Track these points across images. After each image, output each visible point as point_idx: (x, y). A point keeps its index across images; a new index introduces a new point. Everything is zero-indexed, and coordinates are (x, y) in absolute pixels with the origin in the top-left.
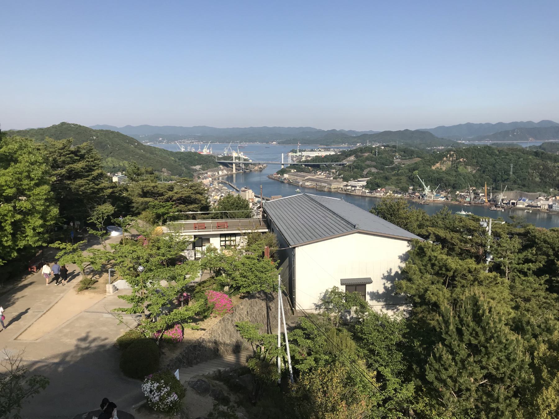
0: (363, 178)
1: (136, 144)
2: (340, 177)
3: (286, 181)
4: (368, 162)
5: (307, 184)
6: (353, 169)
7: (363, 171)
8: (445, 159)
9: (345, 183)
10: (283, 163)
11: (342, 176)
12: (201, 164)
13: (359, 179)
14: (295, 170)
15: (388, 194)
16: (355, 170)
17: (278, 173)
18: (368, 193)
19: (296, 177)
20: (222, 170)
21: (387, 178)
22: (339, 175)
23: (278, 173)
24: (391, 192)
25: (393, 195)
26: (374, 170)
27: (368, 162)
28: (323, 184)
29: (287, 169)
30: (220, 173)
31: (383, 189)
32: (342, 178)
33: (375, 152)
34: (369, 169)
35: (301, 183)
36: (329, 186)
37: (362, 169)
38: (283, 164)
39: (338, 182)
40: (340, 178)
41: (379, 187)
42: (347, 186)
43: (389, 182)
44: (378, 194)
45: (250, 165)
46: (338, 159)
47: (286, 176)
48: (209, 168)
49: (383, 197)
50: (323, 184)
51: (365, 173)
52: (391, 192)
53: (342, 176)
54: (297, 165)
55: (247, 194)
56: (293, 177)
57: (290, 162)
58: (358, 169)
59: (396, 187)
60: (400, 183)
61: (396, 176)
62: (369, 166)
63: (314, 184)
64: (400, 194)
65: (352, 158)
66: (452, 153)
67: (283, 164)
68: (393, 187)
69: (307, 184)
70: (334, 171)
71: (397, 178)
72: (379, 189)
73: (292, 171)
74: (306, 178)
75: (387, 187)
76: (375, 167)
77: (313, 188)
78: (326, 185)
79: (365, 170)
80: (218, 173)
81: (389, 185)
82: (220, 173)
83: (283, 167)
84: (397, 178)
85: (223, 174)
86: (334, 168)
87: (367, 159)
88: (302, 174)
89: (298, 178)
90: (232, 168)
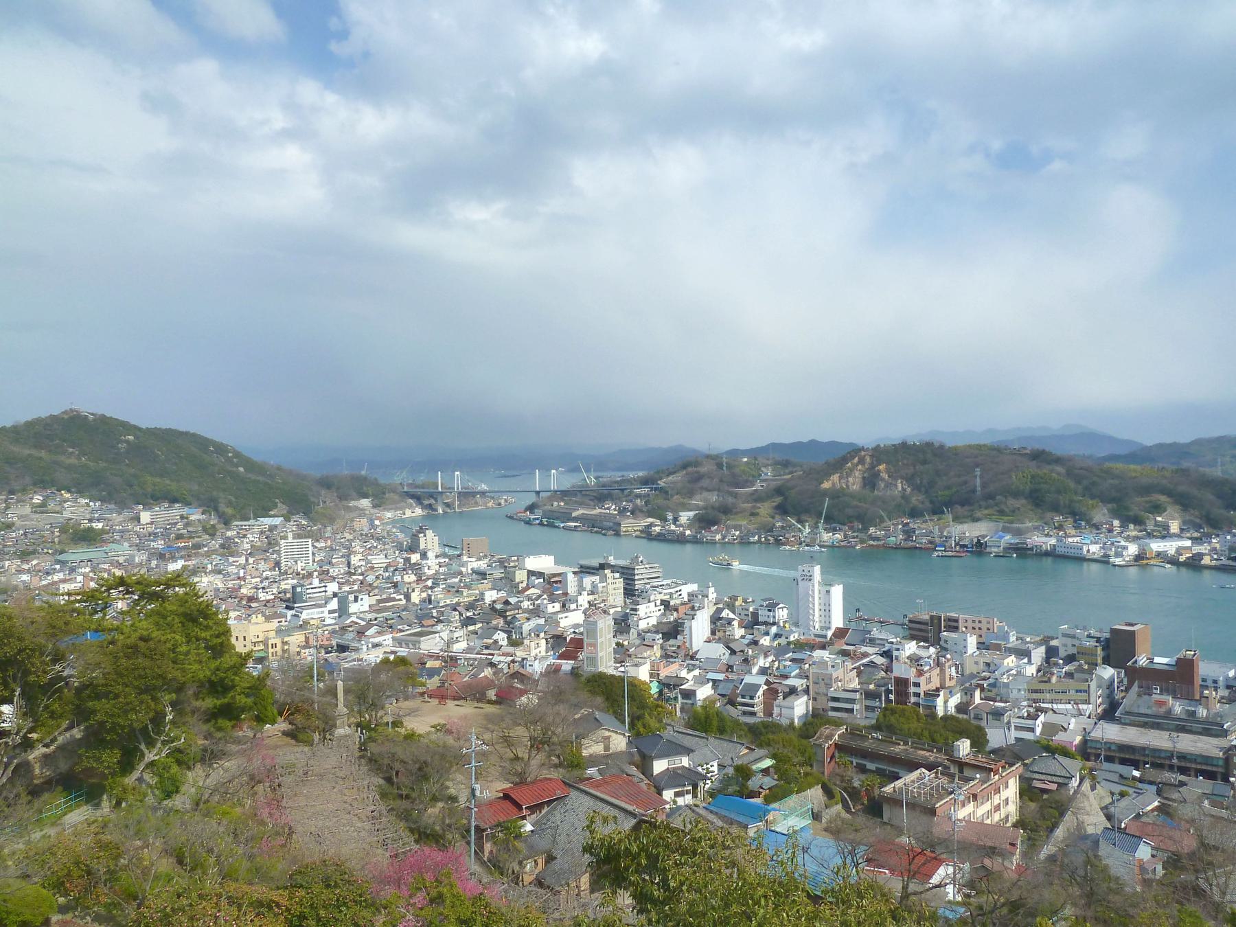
1: (230, 455)
10: (538, 489)
14: (562, 504)
20: (410, 507)
55: (422, 540)
66: (863, 453)
67: (538, 493)
74: (574, 515)
85: (414, 515)
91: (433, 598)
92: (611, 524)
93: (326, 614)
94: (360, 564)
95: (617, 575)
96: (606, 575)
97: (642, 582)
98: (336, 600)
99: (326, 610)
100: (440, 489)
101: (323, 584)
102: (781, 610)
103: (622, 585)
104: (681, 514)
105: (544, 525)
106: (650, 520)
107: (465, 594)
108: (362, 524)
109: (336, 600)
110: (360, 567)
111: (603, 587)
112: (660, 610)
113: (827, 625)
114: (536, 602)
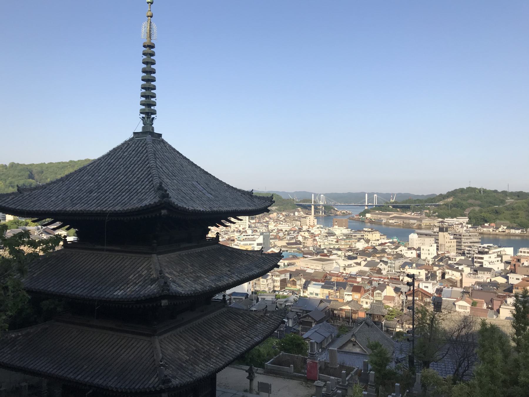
0: (462, 216)
2: (435, 215)
3: (367, 221)
4: (470, 201)
5: (391, 221)
6: (451, 207)
7: (464, 210)
9: (440, 220)
11: (437, 213)
12: (279, 205)
13: (458, 218)
15: (500, 230)
16: (454, 209)
17: (360, 215)
18: (470, 228)
19: (379, 216)
20: (298, 211)
21: (497, 212)
22: (434, 213)
23: (360, 215)
24: (505, 227)
25: (507, 231)
26: (477, 209)
27: (470, 201)
28: (412, 221)
29: (371, 210)
30: (296, 214)
31: (493, 224)
32: (437, 216)
33: (480, 192)
34: (472, 208)
35: (384, 221)
36: (419, 223)
38: (367, 206)
39: (431, 218)
40: (434, 216)
41: (487, 222)
42: (442, 222)
43: (500, 217)
44: (485, 229)
45: (332, 210)
46: (433, 201)
47: (368, 215)
48: (286, 209)
49: (491, 233)
50: (412, 221)
51: (467, 213)
52: (505, 227)
53: (437, 213)
54: (383, 206)
55: (308, 221)
56: (376, 216)
57: (375, 203)
58: (457, 207)
59: (511, 223)
60: (518, 218)
61: (510, 210)
62: (472, 205)
63: (400, 222)
64: (518, 229)
65: (450, 200)
67: (367, 206)
68: (508, 222)
69: (391, 221)
70: (428, 211)
71: (512, 212)
72: (486, 225)
73: (377, 212)
74: (391, 216)
75: (498, 221)
76: (479, 206)
77: (399, 226)
78: (415, 221)
79: (467, 210)
80: (294, 214)
81: (501, 220)
82: (296, 214)
83: (366, 208)
84: (512, 212)
86: (428, 209)
87: (469, 197)
88: (388, 212)
89: (382, 216)
90: (311, 210)
93: (255, 245)
96: (444, 236)
97: (466, 244)
98: (262, 237)
99: (255, 243)
100: (313, 203)
103: (455, 244)
108: (274, 215)
109: (262, 237)
110: (274, 230)
112: (498, 261)
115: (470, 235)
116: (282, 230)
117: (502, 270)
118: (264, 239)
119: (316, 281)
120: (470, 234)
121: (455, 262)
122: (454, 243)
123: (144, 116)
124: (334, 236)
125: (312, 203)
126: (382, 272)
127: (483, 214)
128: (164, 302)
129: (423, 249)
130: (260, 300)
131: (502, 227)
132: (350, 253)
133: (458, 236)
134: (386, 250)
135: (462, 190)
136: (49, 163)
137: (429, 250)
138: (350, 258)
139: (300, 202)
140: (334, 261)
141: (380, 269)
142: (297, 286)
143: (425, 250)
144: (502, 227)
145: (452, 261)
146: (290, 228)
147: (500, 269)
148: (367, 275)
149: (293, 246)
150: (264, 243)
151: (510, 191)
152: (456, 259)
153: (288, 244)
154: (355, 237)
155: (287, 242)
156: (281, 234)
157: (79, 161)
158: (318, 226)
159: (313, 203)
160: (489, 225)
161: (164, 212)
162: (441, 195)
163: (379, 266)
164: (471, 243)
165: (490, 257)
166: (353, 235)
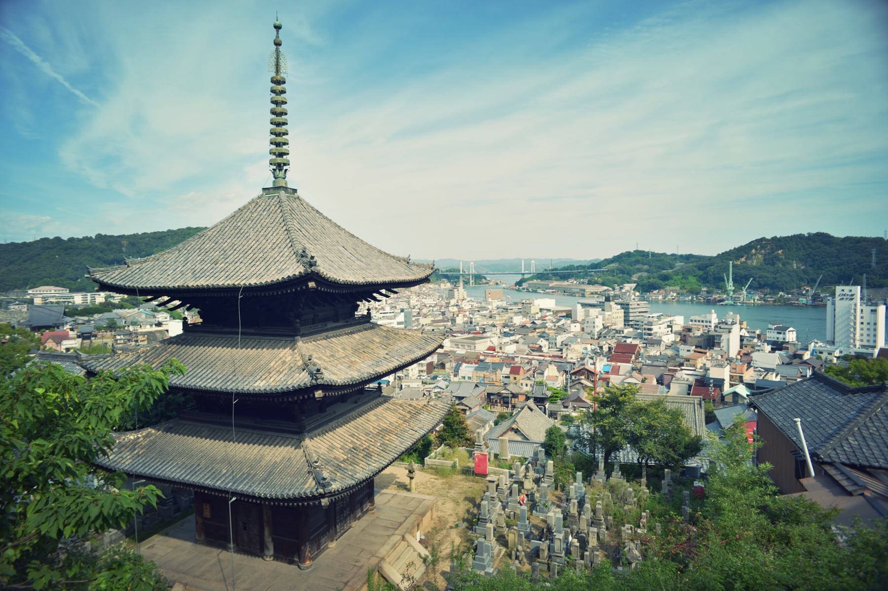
8: (753, 251)
10: (523, 272)
21: (665, 278)
26: (645, 274)
33: (648, 255)
37: (630, 274)
41: (655, 289)
43: (671, 281)
51: (635, 278)
52: (675, 294)
62: (639, 270)
67: (523, 274)
72: (655, 292)
74: (550, 285)
76: (647, 271)
79: (634, 276)
81: (670, 286)
91: (473, 320)
92: (578, 290)
94: (416, 304)
95: (619, 307)
96: (611, 306)
97: (635, 314)
101: (393, 311)
102: (791, 333)
103: (623, 315)
104: (625, 285)
105: (530, 292)
106: (605, 288)
107: (497, 319)
111: (609, 315)
113: (871, 344)
114: (557, 324)
115: (638, 305)
116: (425, 306)
117: (672, 341)
118: (405, 316)
119: (468, 363)
120: (639, 303)
121: (623, 335)
122: (621, 313)
123: (275, 167)
124: (487, 310)
125: (460, 272)
126: (543, 349)
127: (652, 280)
128: (319, 394)
129: (588, 322)
130: (403, 387)
131: (672, 293)
132: (506, 330)
133: (625, 306)
134: (547, 325)
135: (628, 254)
136: (142, 234)
137: (594, 323)
138: (506, 334)
139: (447, 271)
140: (488, 339)
141: (540, 346)
142: (446, 369)
143: (590, 322)
144: (672, 293)
145: (620, 333)
146: (435, 302)
147: (670, 341)
148: (526, 353)
149: (439, 324)
150: (406, 321)
151: (680, 254)
152: (623, 331)
153: (434, 321)
154: (511, 311)
155: (433, 319)
156: (425, 311)
157: (179, 230)
158: (468, 299)
159: (461, 273)
160: (658, 292)
161: (312, 284)
162: (606, 260)
163: (539, 343)
164: (640, 312)
165: (660, 328)
166: (509, 308)
